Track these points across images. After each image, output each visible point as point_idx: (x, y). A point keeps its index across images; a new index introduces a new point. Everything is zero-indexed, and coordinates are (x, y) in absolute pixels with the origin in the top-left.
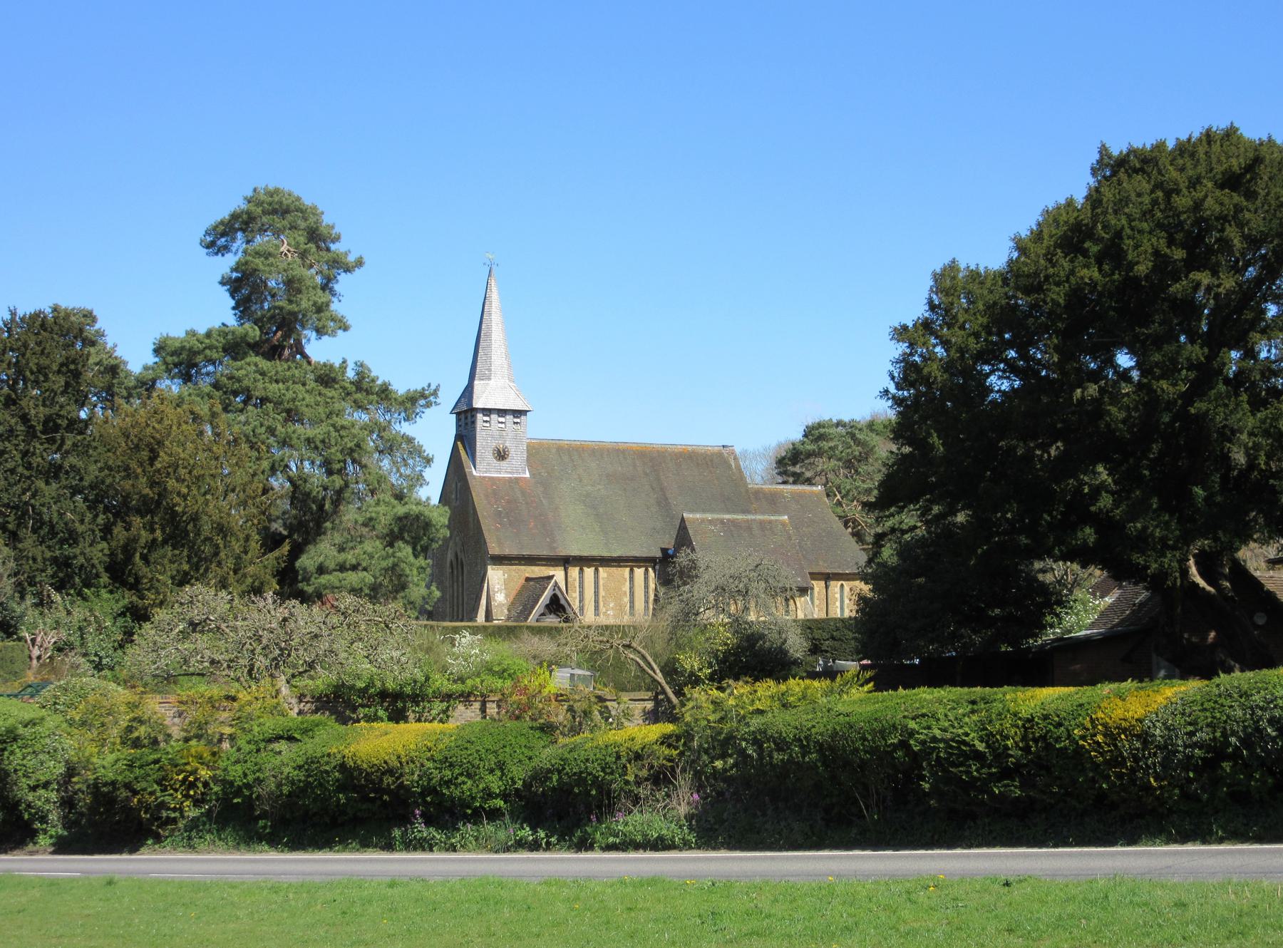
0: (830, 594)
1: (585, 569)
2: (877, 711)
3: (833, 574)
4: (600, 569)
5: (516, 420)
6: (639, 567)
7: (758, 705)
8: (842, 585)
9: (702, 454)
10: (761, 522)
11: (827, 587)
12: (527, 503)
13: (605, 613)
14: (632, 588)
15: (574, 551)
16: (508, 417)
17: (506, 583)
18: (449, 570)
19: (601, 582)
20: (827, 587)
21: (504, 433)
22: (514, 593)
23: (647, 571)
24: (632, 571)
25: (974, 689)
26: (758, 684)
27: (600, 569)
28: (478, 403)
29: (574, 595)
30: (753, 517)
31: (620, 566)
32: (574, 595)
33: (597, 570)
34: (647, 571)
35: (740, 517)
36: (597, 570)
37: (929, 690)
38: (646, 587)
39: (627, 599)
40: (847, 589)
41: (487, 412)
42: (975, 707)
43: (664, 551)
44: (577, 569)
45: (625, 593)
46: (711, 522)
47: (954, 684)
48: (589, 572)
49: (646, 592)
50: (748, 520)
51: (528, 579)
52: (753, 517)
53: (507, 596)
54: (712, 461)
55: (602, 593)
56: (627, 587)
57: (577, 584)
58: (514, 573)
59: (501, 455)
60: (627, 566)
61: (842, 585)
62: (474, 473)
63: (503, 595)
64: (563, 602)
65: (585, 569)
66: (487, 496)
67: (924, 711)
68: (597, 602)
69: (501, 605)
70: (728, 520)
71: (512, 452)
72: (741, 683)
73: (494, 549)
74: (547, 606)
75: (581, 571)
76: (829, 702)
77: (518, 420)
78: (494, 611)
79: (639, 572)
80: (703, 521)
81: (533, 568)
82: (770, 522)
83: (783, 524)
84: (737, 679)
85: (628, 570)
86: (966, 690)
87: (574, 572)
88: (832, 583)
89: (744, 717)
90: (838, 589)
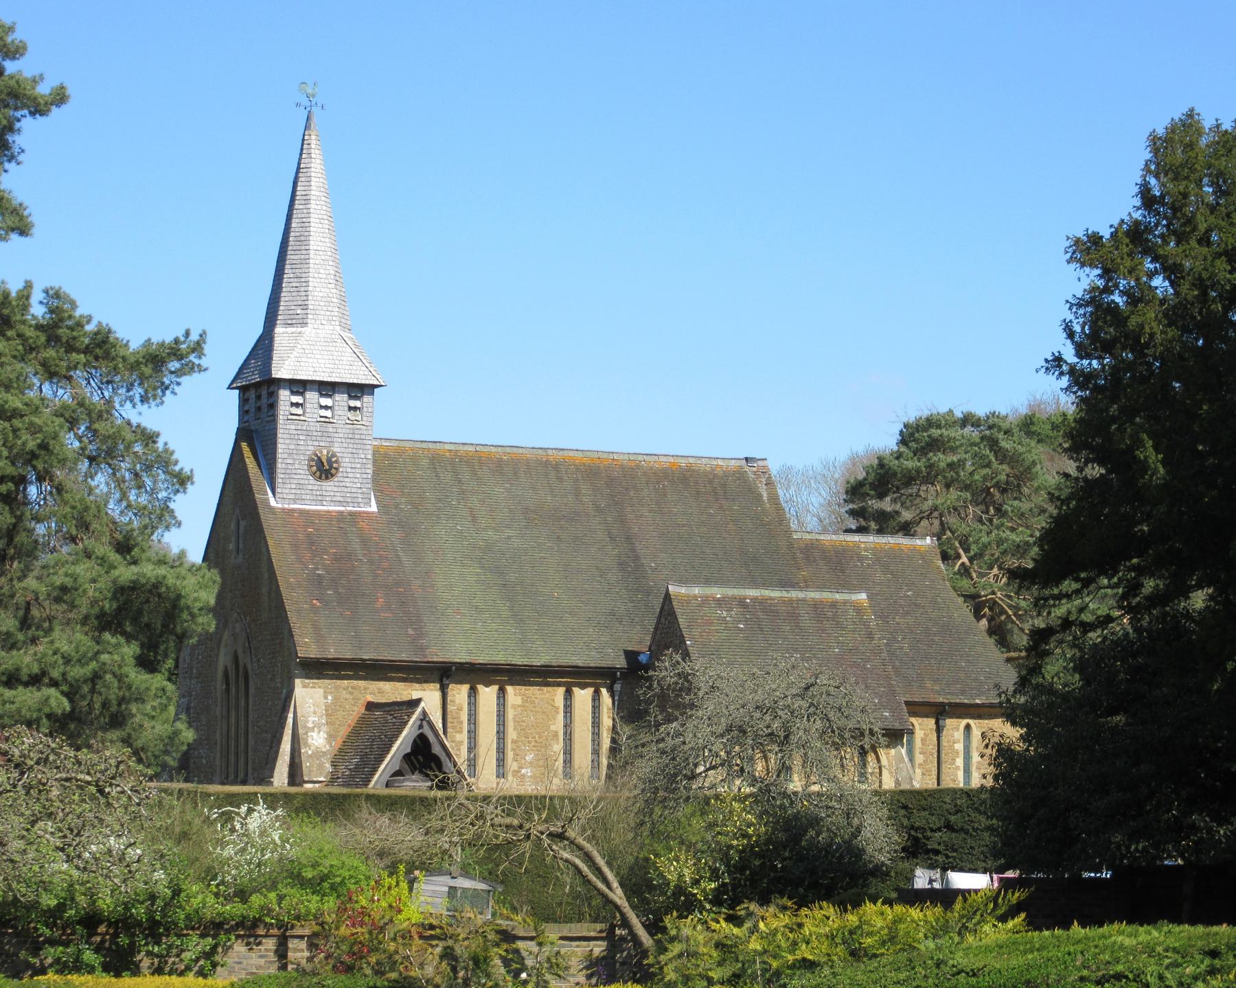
0: (944, 743)
1: (480, 687)
2: (1029, 967)
3: (950, 704)
4: (509, 689)
5: (353, 403)
6: (583, 686)
7: (804, 952)
8: (968, 727)
9: (706, 474)
10: (817, 606)
11: (939, 730)
12: (371, 562)
13: (516, 772)
14: (568, 725)
15: (459, 653)
16: (338, 397)
17: (330, 712)
18: (220, 686)
19: (510, 713)
20: (939, 730)
21: (330, 428)
22: (344, 732)
23: (597, 693)
24: (569, 694)
25: (1215, 929)
26: (804, 911)
27: (509, 689)
28: (281, 370)
29: (458, 737)
30: (801, 595)
31: (547, 684)
32: (458, 737)
33: (502, 691)
34: (597, 693)
35: (776, 594)
36: (502, 691)
37: (1130, 929)
38: (596, 723)
39: (558, 747)
40: (976, 734)
41: (298, 386)
42: (1217, 963)
43: (631, 656)
44: (465, 688)
45: (556, 735)
46: (720, 603)
47: (1178, 920)
48: (488, 694)
49: (596, 735)
50: (791, 601)
51: (370, 706)
52: (801, 595)
53: (331, 737)
54: (724, 486)
55: (511, 734)
56: (558, 724)
57: (464, 717)
58: (344, 694)
59: (324, 469)
60: (559, 685)
61: (968, 727)
62: (273, 502)
63: (323, 735)
64: (436, 749)
65: (480, 687)
66: (295, 546)
67: (1120, 968)
68: (501, 751)
69: (318, 754)
70: (754, 599)
72: (772, 909)
73: (307, 647)
74: (407, 758)
75: (473, 692)
76: (939, 948)
77: (357, 404)
78: (306, 764)
79: (583, 696)
80: (705, 600)
81: (381, 684)
82: (834, 604)
83: (858, 609)
84: (764, 901)
85: (561, 691)
86: (1200, 929)
87: (459, 693)
88: (950, 723)
89: (778, 974)
90: (959, 735)
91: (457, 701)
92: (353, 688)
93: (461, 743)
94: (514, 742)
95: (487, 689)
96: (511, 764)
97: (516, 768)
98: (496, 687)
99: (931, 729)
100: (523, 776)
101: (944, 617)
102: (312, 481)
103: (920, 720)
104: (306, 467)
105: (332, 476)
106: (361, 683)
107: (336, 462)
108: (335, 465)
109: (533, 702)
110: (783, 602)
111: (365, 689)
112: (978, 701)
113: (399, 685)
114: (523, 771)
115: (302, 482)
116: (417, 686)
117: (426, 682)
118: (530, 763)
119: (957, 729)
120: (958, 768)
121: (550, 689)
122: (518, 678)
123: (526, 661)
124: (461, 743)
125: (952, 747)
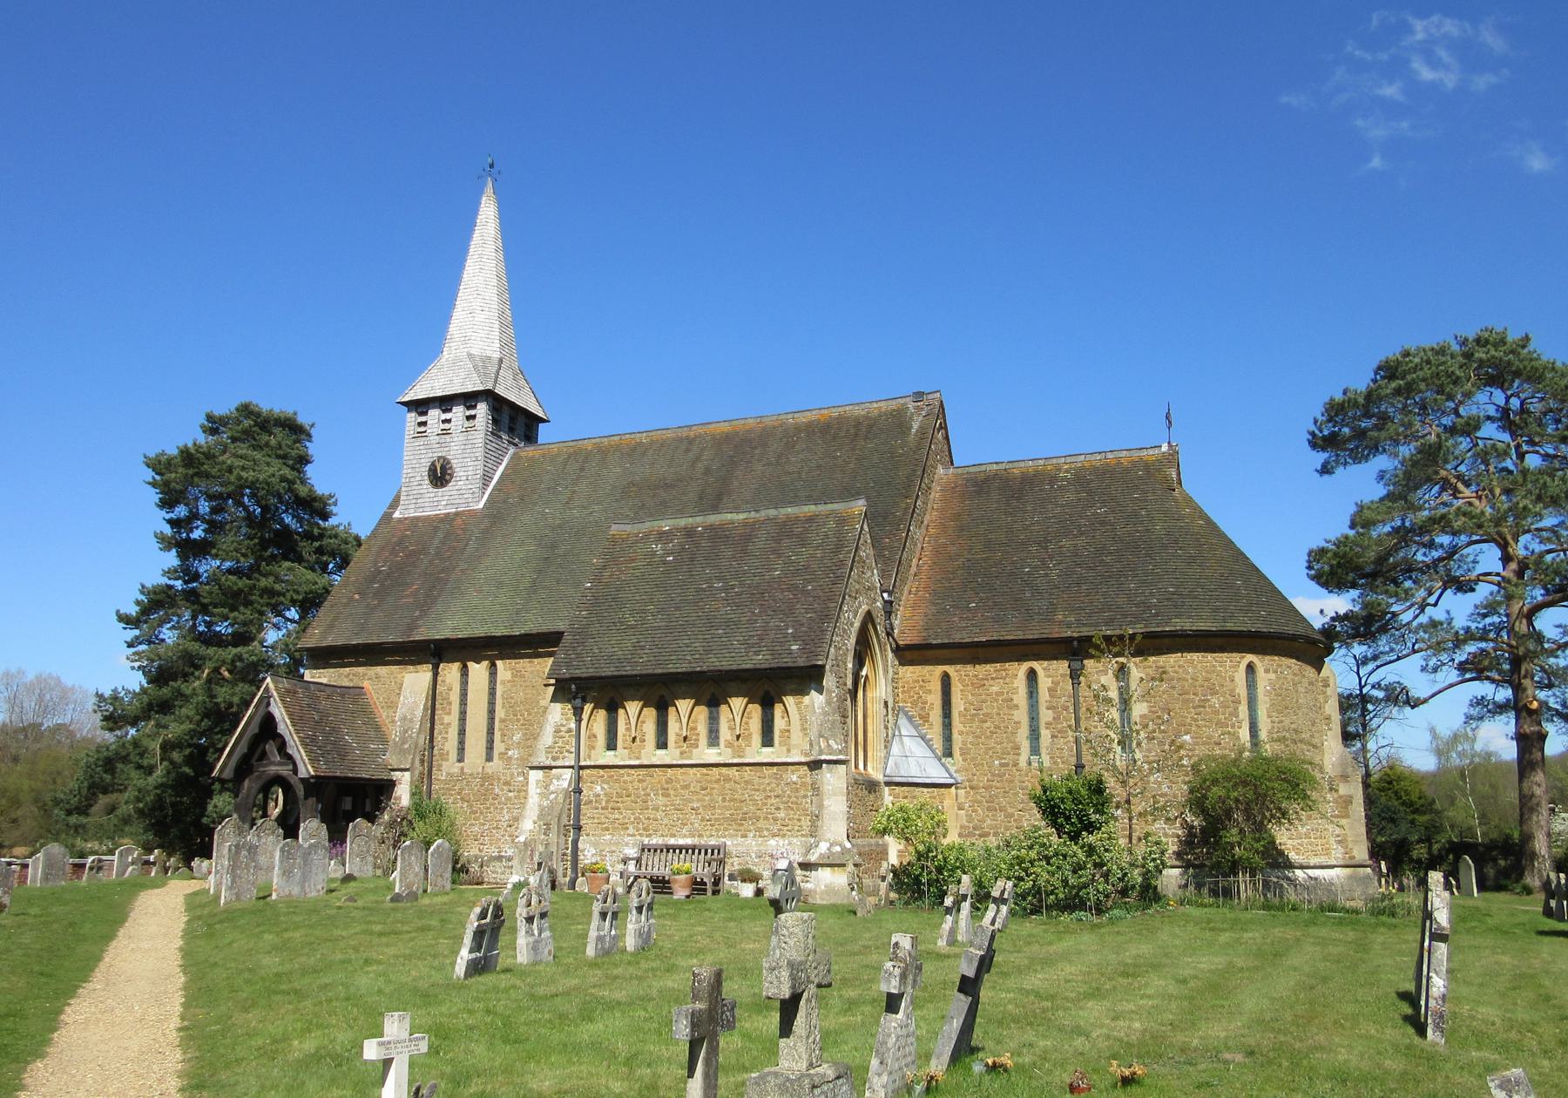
4: (499, 663)
5: (469, 413)
12: (437, 554)
19: (499, 689)
20: (1075, 675)
27: (499, 663)
29: (447, 719)
32: (447, 719)
33: (493, 665)
44: (456, 666)
46: (662, 536)
48: (478, 670)
52: (772, 512)
55: (500, 713)
57: (455, 697)
71: (459, 473)
75: (464, 672)
87: (450, 672)
90: (1108, 679)
91: (448, 681)
92: (354, 675)
93: (449, 724)
94: (502, 721)
95: (477, 666)
96: (499, 747)
97: (503, 751)
98: (485, 663)
99: (1062, 675)
100: (510, 758)
101: (1137, 531)
102: (431, 490)
103: (1046, 663)
104: (426, 478)
105: (448, 482)
106: (361, 670)
107: (451, 468)
108: (449, 472)
109: (523, 676)
110: (745, 524)
111: (364, 675)
113: (393, 668)
114: (510, 753)
115: (422, 491)
116: (411, 668)
117: (420, 663)
118: (519, 743)
121: (540, 660)
122: (508, 651)
123: (506, 632)
124: (449, 724)
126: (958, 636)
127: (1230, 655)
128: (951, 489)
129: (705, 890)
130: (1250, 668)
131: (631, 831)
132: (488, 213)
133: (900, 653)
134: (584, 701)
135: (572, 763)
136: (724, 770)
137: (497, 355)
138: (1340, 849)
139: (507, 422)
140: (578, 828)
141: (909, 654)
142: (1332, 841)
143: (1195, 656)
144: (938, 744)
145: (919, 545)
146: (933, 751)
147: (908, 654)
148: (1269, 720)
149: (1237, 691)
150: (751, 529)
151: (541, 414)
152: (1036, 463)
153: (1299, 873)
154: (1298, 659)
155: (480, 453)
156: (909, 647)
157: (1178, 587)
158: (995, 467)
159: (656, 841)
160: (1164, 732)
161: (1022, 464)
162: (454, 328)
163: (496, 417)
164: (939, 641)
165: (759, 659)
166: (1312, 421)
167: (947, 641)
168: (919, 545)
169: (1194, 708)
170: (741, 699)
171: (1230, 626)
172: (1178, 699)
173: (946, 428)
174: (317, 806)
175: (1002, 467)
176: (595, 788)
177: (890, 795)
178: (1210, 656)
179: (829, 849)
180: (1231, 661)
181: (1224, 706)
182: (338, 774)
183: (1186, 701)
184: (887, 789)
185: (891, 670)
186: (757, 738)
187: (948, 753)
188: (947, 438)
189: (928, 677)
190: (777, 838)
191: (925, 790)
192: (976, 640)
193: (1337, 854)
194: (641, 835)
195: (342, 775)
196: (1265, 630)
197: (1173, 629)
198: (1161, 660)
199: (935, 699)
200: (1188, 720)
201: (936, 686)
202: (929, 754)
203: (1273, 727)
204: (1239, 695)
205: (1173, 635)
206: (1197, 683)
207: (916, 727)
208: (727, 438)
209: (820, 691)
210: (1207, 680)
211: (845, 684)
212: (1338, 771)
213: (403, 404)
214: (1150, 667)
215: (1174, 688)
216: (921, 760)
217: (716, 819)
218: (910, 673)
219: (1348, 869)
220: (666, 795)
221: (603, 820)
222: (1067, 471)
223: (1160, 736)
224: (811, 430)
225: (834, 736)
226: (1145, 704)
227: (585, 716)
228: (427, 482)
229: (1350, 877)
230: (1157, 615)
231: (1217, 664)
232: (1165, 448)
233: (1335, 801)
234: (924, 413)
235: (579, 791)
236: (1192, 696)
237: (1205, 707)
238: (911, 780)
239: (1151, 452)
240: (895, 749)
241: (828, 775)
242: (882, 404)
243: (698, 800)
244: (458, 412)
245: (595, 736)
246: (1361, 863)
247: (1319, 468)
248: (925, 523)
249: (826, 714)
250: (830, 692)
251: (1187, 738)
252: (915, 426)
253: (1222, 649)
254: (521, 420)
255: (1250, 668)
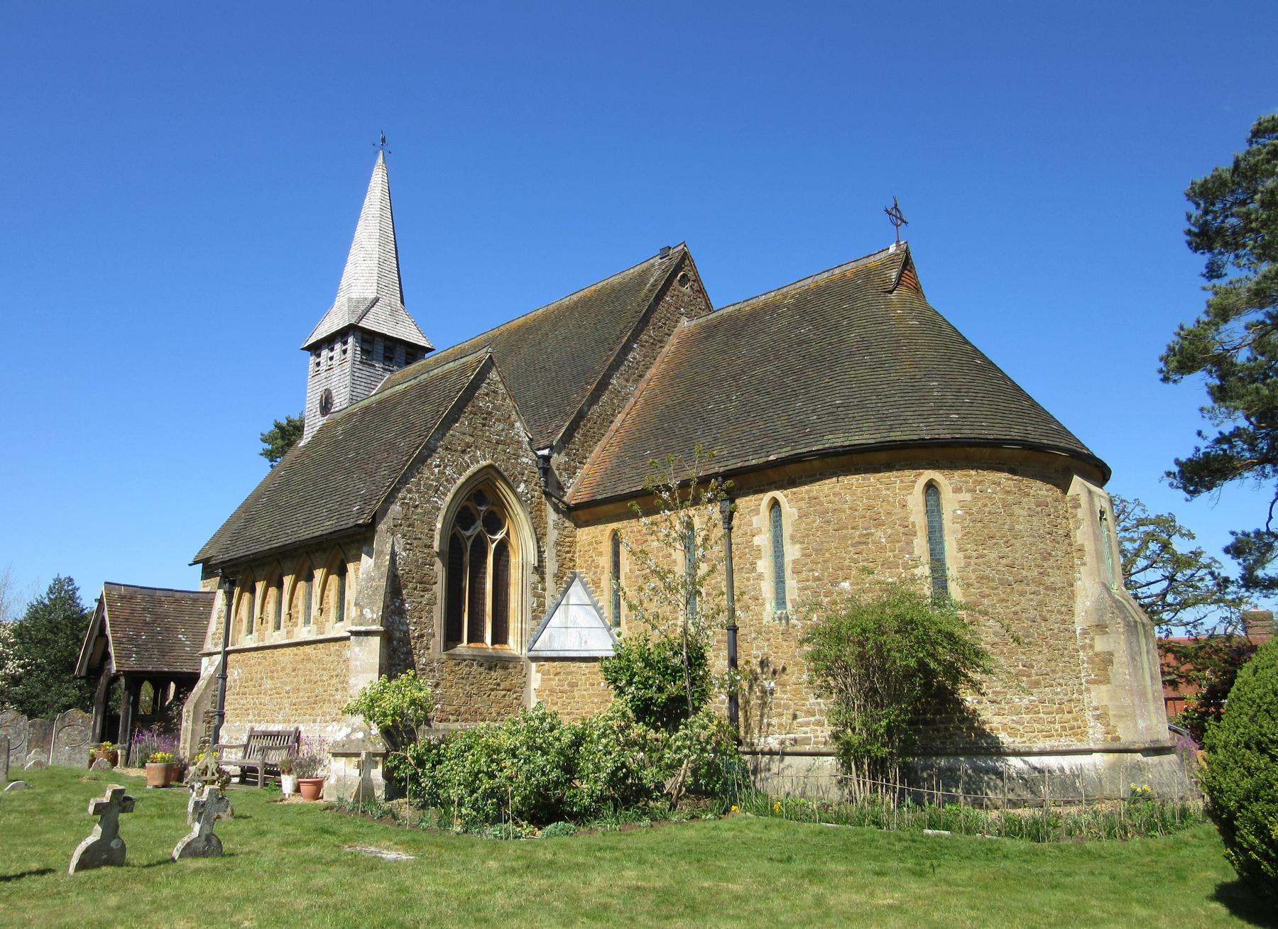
8: (775, 504)
11: (729, 518)
40: (789, 511)
61: (775, 504)
90: (762, 520)
101: (830, 344)
112: (772, 458)
119: (757, 512)
120: (760, 576)
125: (749, 544)
126: (621, 488)
127: (900, 473)
128: (692, 341)
129: (257, 783)
130: (931, 487)
131: (250, 717)
132: (378, 179)
133: (574, 513)
134: (233, 584)
135: (220, 648)
136: (308, 649)
137: (373, 296)
138: (1100, 728)
139: (382, 352)
140: (222, 716)
141: (583, 513)
142: (1088, 715)
143: (854, 480)
144: (608, 613)
145: (632, 400)
146: (603, 621)
147: (581, 514)
148: (961, 555)
149: (911, 519)
150: (405, 393)
151: (423, 342)
152: (768, 296)
153: (1015, 762)
154: (1013, 471)
155: (348, 380)
156: (579, 507)
157: (848, 397)
158: (731, 309)
159: (260, 727)
160: (818, 579)
161: (754, 301)
162: (344, 282)
163: (365, 347)
164: (604, 496)
165: (327, 526)
166: (1185, 217)
167: (609, 495)
168: (632, 400)
169: (853, 545)
170: (322, 569)
171: (896, 436)
172: (833, 536)
173: (697, 280)
174: (129, 698)
175: (737, 307)
176: (234, 674)
177: (538, 672)
178: (872, 478)
179: (348, 736)
180: (902, 481)
181: (892, 539)
182: (150, 669)
183: (845, 537)
184: (534, 665)
185: (552, 535)
186: (333, 613)
187: (618, 624)
188: (701, 291)
189: (600, 538)
190: (334, 723)
191: (583, 665)
192: (634, 489)
193: (1095, 735)
194: (256, 721)
195: (154, 670)
196: (948, 436)
197: (820, 447)
198: (816, 489)
199: (605, 561)
200: (847, 563)
201: (607, 547)
202: (599, 623)
203: (968, 565)
204: (914, 524)
205: (824, 455)
206: (857, 513)
207: (589, 594)
208: (519, 328)
209: (370, 556)
210: (869, 508)
211: (431, 547)
212: (1093, 620)
213: (303, 349)
214: (803, 499)
215: (828, 522)
216: (585, 632)
217: (300, 703)
218: (584, 535)
219: (1111, 755)
220: (272, 678)
221: (237, 706)
222: (791, 298)
223: (814, 585)
224: (572, 308)
225: (371, 604)
226: (798, 546)
227: (235, 601)
228: (319, 413)
229: (1113, 767)
230: (810, 433)
231: (883, 487)
232: (892, 248)
233: (1091, 661)
234: (663, 267)
235: (224, 677)
236: (850, 531)
237: (866, 543)
238: (562, 654)
239: (878, 257)
240: (556, 620)
241: (357, 649)
242: (636, 269)
243: (292, 682)
244: (338, 347)
245: (241, 620)
246: (1127, 746)
247: (1205, 271)
248: (648, 376)
249: (371, 579)
250: (381, 553)
251: (846, 585)
252: (652, 280)
253: (889, 467)
254: (400, 353)
255: (931, 487)
